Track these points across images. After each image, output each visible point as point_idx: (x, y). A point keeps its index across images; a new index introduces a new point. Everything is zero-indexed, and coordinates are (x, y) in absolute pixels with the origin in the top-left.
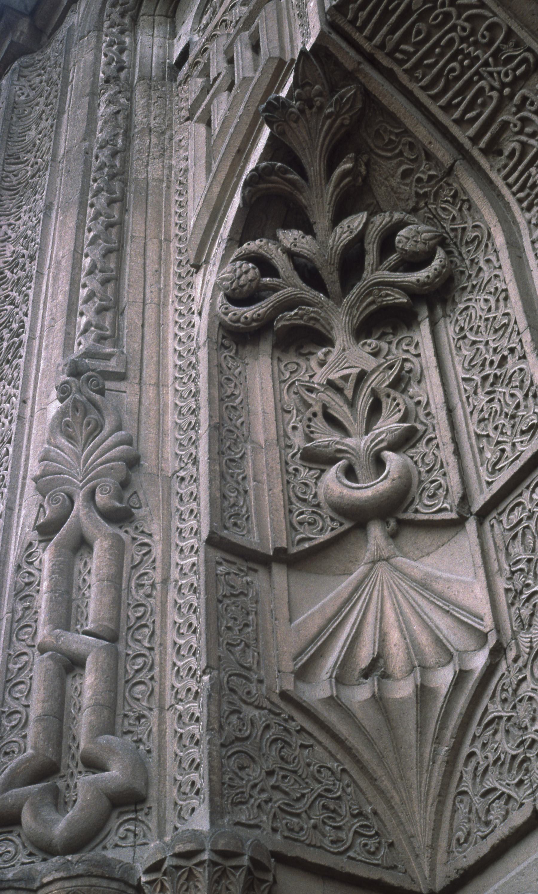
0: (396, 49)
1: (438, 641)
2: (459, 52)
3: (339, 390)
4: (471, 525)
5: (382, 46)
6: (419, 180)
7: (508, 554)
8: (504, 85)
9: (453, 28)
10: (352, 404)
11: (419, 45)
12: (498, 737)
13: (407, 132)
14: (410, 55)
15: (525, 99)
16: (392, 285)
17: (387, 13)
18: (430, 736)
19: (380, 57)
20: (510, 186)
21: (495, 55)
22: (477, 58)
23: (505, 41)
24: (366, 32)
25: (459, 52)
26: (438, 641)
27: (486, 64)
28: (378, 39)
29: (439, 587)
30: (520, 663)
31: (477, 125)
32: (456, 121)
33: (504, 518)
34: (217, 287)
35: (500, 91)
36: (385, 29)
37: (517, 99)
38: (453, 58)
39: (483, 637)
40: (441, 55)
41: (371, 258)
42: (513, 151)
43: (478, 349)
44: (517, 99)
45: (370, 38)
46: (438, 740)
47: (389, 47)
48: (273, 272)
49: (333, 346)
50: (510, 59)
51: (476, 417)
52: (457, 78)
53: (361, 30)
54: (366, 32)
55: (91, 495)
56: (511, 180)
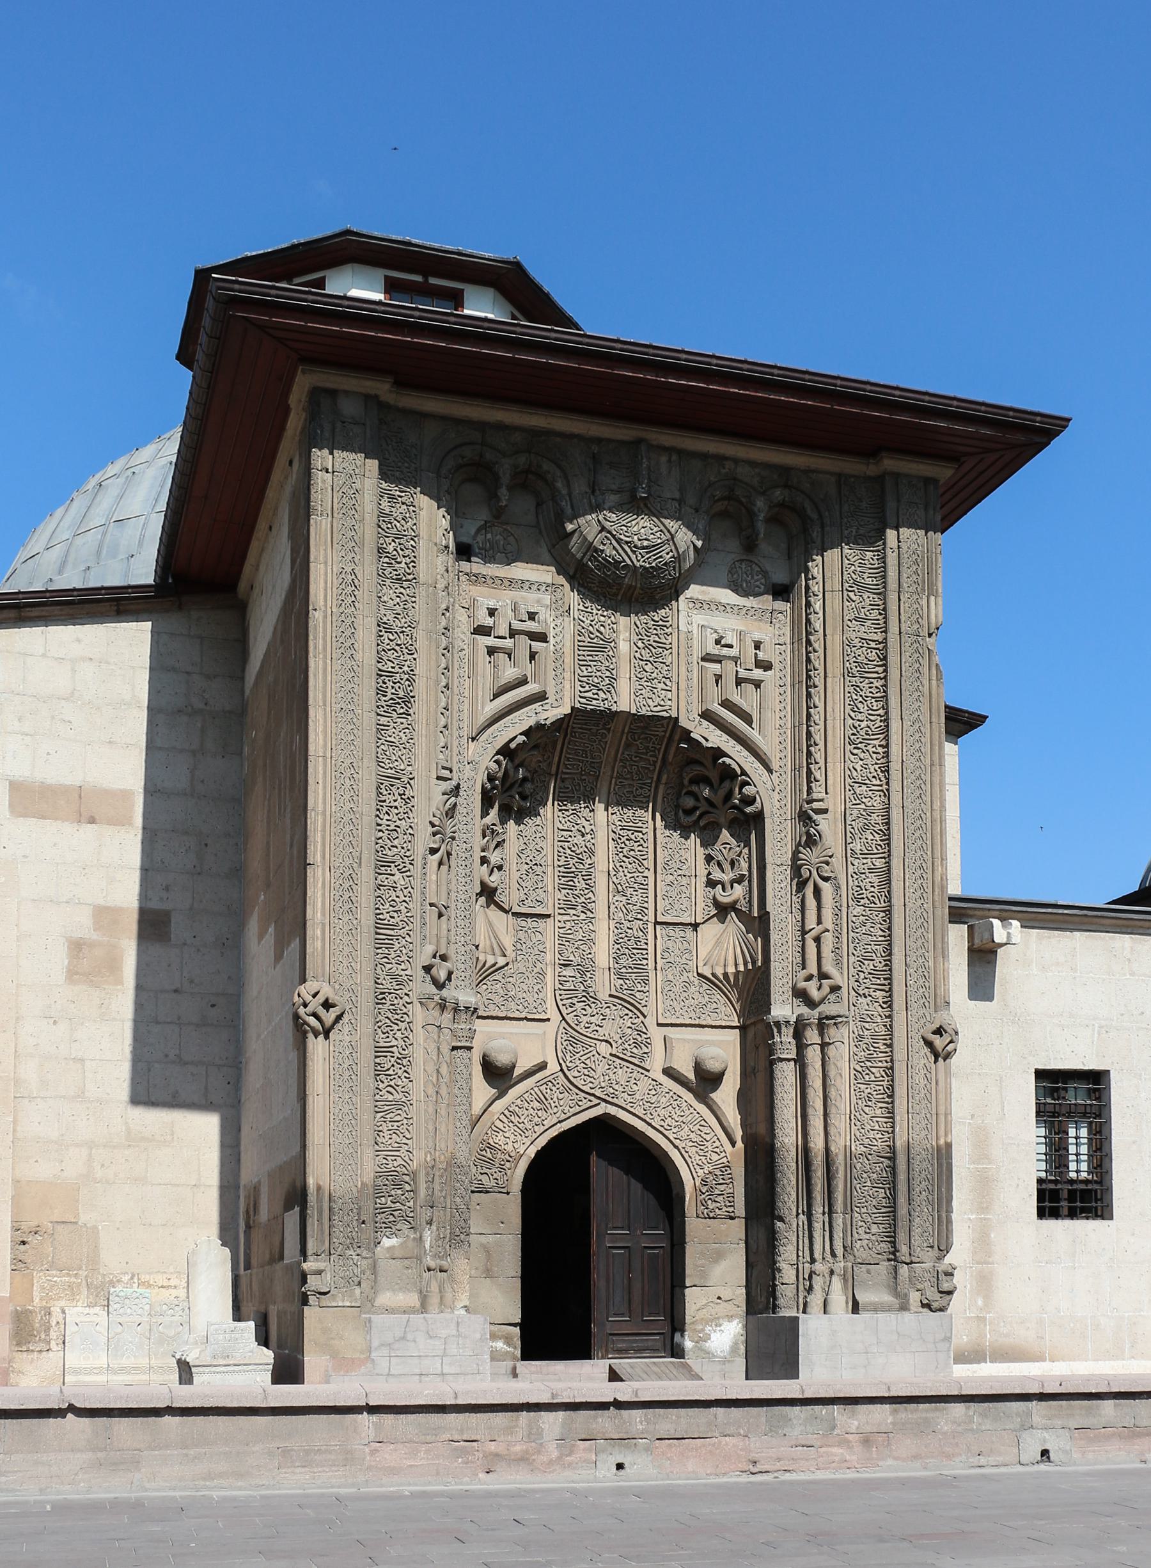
0: (575, 732)
2: (586, 751)
5: (573, 728)
6: (540, 766)
9: (592, 745)
13: (553, 754)
14: (575, 737)
19: (570, 728)
24: (575, 721)
25: (586, 751)
27: (587, 761)
28: (575, 726)
29: (495, 928)
30: (512, 971)
31: (568, 771)
32: (564, 763)
35: (582, 771)
36: (579, 726)
37: (583, 777)
42: (568, 788)
44: (583, 777)
45: (574, 723)
46: (480, 976)
47: (575, 730)
50: (594, 768)
51: (519, 874)
52: (577, 756)
53: (575, 719)
54: (575, 721)
56: (561, 795)
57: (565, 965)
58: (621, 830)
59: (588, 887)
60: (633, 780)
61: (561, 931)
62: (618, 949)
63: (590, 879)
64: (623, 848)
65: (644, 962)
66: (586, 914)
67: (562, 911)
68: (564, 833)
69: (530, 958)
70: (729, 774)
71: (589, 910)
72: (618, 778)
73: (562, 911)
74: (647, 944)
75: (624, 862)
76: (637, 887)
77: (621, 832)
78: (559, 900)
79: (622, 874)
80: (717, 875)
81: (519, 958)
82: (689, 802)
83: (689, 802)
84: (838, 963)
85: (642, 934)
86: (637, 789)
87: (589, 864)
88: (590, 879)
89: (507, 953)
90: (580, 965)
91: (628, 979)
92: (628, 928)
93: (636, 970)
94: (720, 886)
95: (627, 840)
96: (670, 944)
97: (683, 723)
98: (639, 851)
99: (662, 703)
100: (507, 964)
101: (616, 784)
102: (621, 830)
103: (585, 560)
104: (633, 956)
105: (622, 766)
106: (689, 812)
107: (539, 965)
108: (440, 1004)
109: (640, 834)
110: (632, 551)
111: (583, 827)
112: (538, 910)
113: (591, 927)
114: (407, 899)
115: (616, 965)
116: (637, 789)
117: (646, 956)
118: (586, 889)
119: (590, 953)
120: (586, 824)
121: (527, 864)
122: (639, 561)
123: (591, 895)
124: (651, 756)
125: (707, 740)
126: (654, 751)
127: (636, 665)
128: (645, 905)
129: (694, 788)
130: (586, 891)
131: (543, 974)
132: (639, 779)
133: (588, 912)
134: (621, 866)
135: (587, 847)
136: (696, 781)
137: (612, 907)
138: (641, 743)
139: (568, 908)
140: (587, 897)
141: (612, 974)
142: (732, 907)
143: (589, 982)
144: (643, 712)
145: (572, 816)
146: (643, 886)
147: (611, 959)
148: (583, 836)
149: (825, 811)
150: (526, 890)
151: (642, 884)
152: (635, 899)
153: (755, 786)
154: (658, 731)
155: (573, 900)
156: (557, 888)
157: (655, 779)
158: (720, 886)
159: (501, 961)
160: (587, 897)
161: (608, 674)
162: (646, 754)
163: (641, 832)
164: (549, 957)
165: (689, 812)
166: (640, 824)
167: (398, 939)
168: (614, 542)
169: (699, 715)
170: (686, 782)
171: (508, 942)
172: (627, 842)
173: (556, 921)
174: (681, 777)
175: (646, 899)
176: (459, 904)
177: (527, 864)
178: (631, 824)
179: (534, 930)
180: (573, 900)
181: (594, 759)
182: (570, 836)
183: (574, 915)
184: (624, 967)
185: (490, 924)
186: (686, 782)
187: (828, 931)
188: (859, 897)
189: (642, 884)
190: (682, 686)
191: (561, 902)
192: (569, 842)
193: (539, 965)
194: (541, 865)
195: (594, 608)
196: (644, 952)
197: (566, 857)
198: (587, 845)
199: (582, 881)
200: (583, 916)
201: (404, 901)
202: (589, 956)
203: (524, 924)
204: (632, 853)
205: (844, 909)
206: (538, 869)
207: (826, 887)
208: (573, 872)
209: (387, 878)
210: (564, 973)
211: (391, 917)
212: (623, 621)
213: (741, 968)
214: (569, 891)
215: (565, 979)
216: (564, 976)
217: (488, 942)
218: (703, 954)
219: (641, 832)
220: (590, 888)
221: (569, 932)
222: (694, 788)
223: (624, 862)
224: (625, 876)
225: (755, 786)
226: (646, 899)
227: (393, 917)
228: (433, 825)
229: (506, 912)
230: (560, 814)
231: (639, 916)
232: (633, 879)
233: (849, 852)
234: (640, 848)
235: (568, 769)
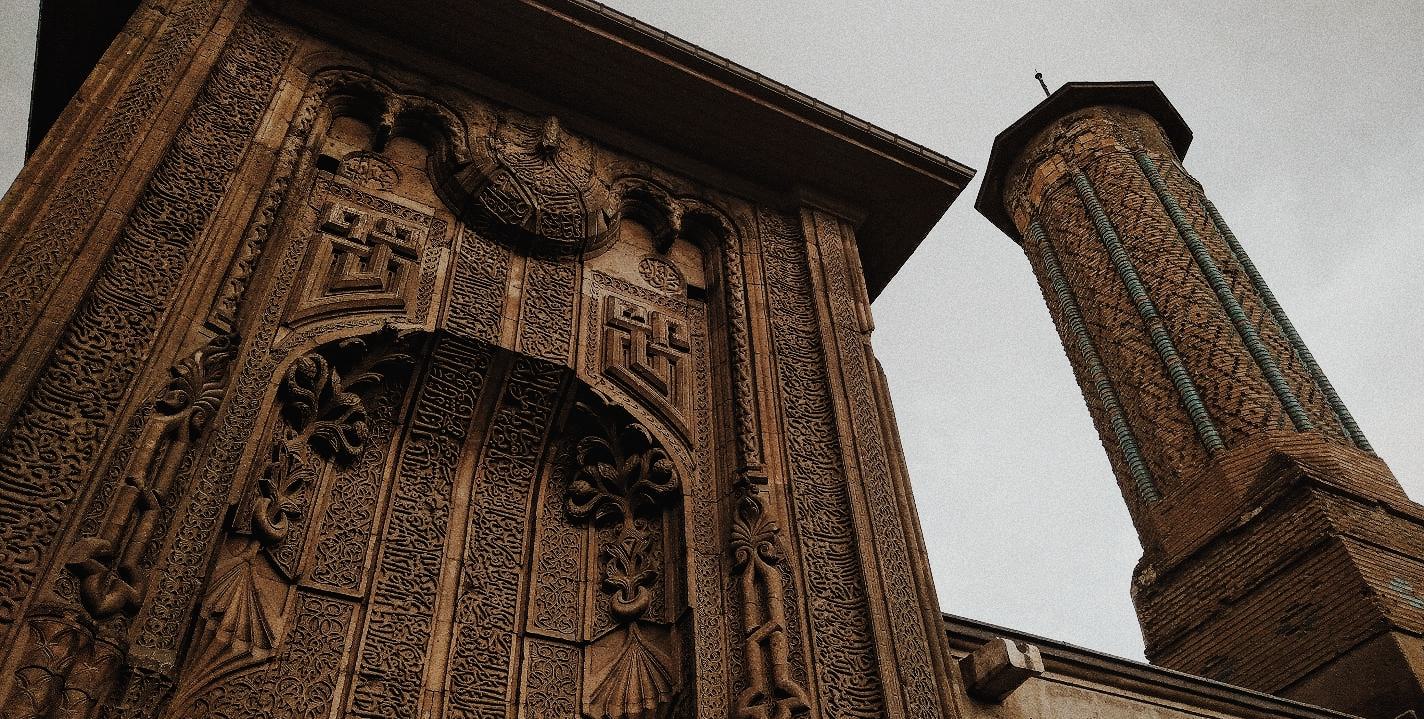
1: (248, 626)
2: (450, 399)
3: (291, 464)
4: (293, 589)
6: (383, 409)
7: (299, 620)
8: (445, 428)
9: (459, 392)
10: (289, 473)
11: (444, 378)
12: (243, 694)
14: (438, 376)
15: (445, 441)
16: (340, 439)
17: (453, 358)
18: (213, 666)
20: (405, 457)
21: (457, 418)
22: (451, 410)
23: (464, 419)
26: (248, 626)
27: (451, 415)
29: (262, 600)
30: (276, 674)
33: (308, 600)
34: (298, 361)
38: (446, 398)
39: (267, 646)
40: (444, 391)
41: (344, 418)
42: (419, 449)
43: (343, 509)
46: (213, 671)
48: (317, 378)
49: (299, 431)
52: (437, 404)
55: (195, 412)
57: (369, 677)
58: (487, 512)
59: (426, 573)
60: (511, 453)
61: (375, 626)
62: (462, 665)
63: (434, 565)
64: (487, 535)
65: (501, 689)
66: (419, 608)
67: (380, 599)
68: (404, 502)
69: (312, 659)
70: (640, 443)
71: (422, 603)
72: (490, 446)
73: (380, 599)
74: (507, 663)
75: (487, 552)
76: (501, 586)
77: (487, 516)
78: (380, 583)
79: (482, 566)
80: (616, 578)
81: (294, 656)
82: (584, 486)
83: (584, 486)
84: (800, 675)
85: (500, 647)
86: (514, 467)
87: (435, 546)
88: (434, 565)
89: (276, 644)
90: (396, 680)
91: (472, 712)
92: (481, 637)
93: (485, 700)
94: (619, 592)
95: (494, 525)
96: (542, 669)
97: (582, 374)
98: (509, 541)
99: (556, 352)
100: (270, 660)
101: (487, 456)
102: (487, 512)
103: (476, 195)
104: (483, 677)
105: (496, 430)
106: (581, 499)
107: (326, 672)
108: (75, 633)
109: (514, 524)
110: (533, 193)
111: (434, 500)
112: (345, 591)
113: (423, 628)
114: (81, 455)
115: (455, 688)
116: (514, 467)
117: (504, 681)
118: (426, 575)
119: (416, 665)
120: (439, 498)
121: (340, 528)
122: (539, 204)
123: (430, 585)
124: (537, 421)
125: (610, 400)
126: (540, 415)
127: (528, 310)
128: (511, 610)
129: (590, 469)
130: (424, 579)
131: (330, 684)
132: (518, 454)
133: (423, 608)
134: (481, 555)
135: (435, 525)
136: (592, 460)
137: (461, 607)
138: (525, 400)
139: (392, 597)
140: (425, 586)
141: (446, 699)
142: (637, 617)
143: (406, 708)
144: (532, 354)
145: (420, 486)
146: (511, 585)
147: (448, 678)
148: (432, 510)
149: (764, 481)
150: (330, 561)
151: (510, 583)
152: (495, 600)
153: (671, 459)
154: (548, 385)
155: (402, 587)
156: (379, 566)
157: (539, 456)
158: (619, 592)
159: (259, 654)
160: (425, 586)
161: (490, 309)
162: (529, 417)
163: (515, 520)
164: (345, 660)
165: (581, 499)
166: (514, 511)
167: (33, 511)
168: (512, 179)
169: (601, 374)
170: (580, 458)
171: (278, 626)
172: (494, 529)
173: (370, 612)
174: (575, 453)
175: (513, 603)
176: (194, 517)
177: (340, 528)
178: (502, 509)
179: (330, 618)
180: (402, 587)
181: (460, 413)
182: (413, 508)
183: (399, 607)
184: (468, 692)
185: (256, 594)
186: (580, 458)
187: (780, 630)
188: (820, 586)
189: (510, 583)
190: (583, 342)
191: (382, 586)
192: (410, 513)
193: (326, 672)
194: (360, 533)
195: (481, 246)
196: (503, 675)
197: (401, 531)
198: (437, 522)
199: (421, 566)
200: (413, 611)
201: (74, 457)
202: (414, 669)
203: (314, 607)
204: (499, 542)
205: (801, 601)
206: (357, 539)
207: (774, 574)
208: (409, 552)
209: (54, 419)
210: (367, 689)
211: (34, 474)
212: (516, 268)
213: (650, 705)
214: (398, 575)
215: (365, 698)
216: (366, 694)
217: (242, 621)
218: (591, 684)
219: (515, 520)
220: (433, 577)
221: (386, 629)
222: (590, 469)
223: (487, 552)
224: (487, 569)
225: (671, 459)
226: (513, 603)
227: (39, 476)
228: (174, 372)
229: (288, 582)
230: (403, 479)
231: (500, 624)
232: (496, 575)
233: (800, 529)
234: (512, 539)
235: (423, 421)
